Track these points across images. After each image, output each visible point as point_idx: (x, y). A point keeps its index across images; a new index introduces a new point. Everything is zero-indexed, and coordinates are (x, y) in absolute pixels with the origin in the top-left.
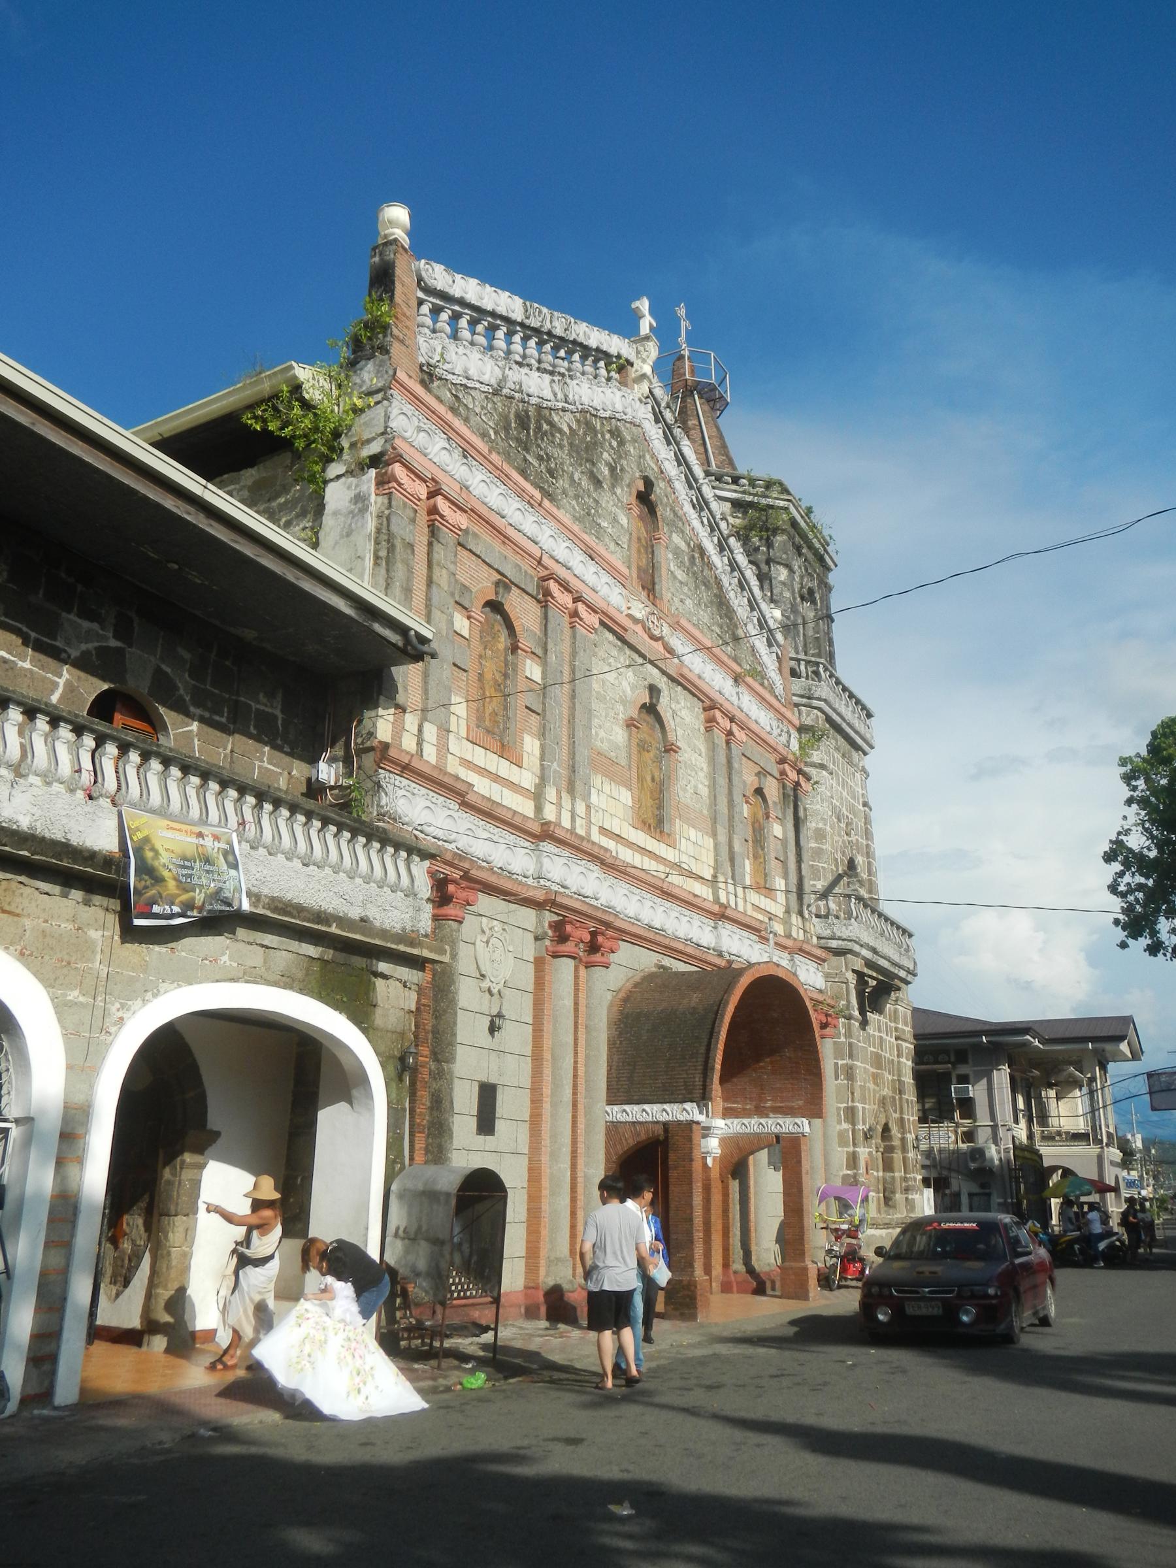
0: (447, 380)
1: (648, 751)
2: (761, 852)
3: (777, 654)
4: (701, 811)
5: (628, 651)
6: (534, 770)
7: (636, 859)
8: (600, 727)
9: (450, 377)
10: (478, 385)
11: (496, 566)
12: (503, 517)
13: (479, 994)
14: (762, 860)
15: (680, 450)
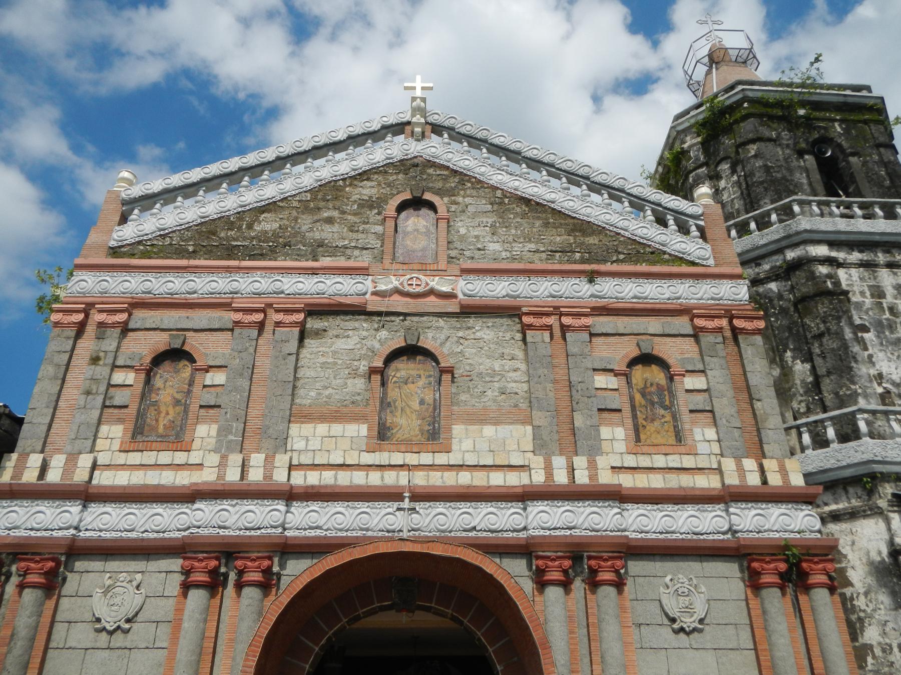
0: (141, 241)
1: (413, 383)
2: (662, 412)
3: (697, 226)
4: (516, 406)
5: (377, 319)
6: (209, 448)
7: (375, 479)
8: (326, 388)
9: (145, 238)
10: (175, 228)
11: (174, 327)
12: (195, 292)
13: (93, 634)
14: (668, 418)
15: (491, 144)
